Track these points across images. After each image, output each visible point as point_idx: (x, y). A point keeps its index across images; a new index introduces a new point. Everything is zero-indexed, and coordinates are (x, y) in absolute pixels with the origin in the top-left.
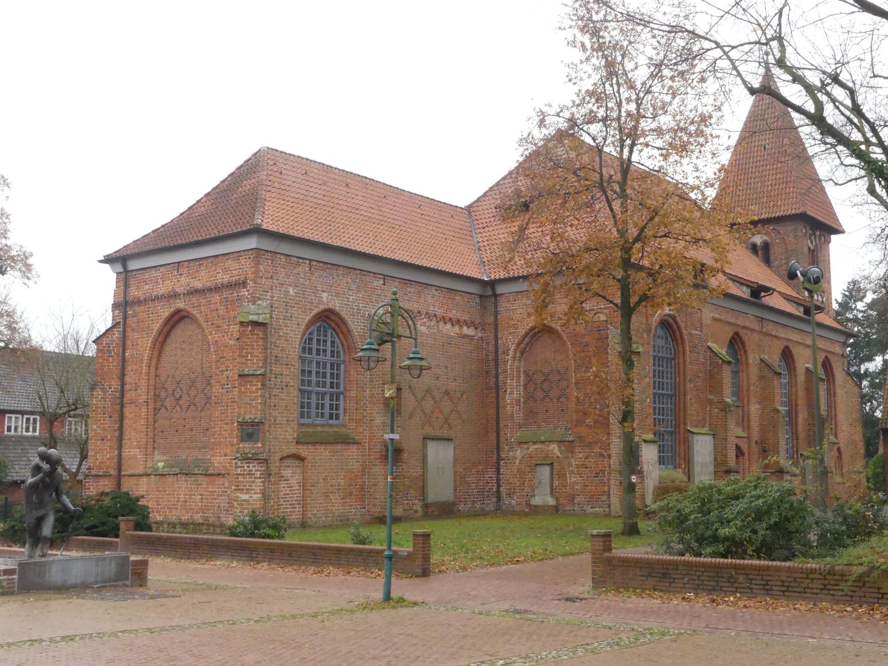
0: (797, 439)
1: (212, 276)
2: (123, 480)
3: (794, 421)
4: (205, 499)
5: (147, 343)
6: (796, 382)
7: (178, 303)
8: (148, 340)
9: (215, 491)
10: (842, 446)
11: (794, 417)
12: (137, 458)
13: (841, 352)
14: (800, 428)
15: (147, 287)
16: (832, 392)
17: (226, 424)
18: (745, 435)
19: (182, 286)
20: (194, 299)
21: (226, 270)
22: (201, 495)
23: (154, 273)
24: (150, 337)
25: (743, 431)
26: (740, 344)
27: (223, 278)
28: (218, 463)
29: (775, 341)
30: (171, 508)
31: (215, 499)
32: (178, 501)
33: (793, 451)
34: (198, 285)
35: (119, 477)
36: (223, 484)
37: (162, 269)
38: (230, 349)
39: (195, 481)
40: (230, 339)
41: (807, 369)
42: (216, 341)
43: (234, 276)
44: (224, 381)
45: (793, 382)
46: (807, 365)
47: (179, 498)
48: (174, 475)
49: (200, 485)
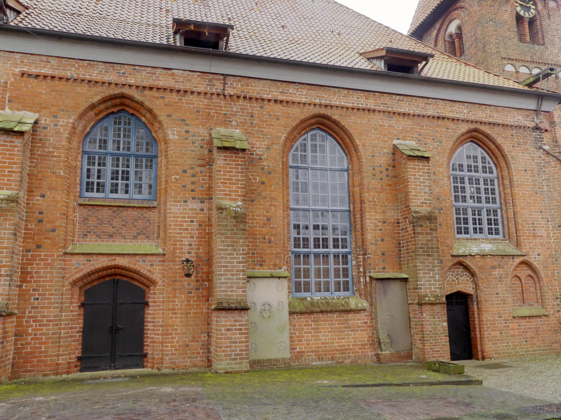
0: (365, 254)
3: (359, 227)
6: (361, 167)
10: (534, 259)
11: (358, 220)
13: (533, 125)
14: (369, 237)
16: (507, 182)
18: (160, 251)
25: (157, 246)
26: (148, 115)
29: (279, 106)
33: (359, 272)
41: (395, 147)
45: (356, 168)
46: (395, 142)
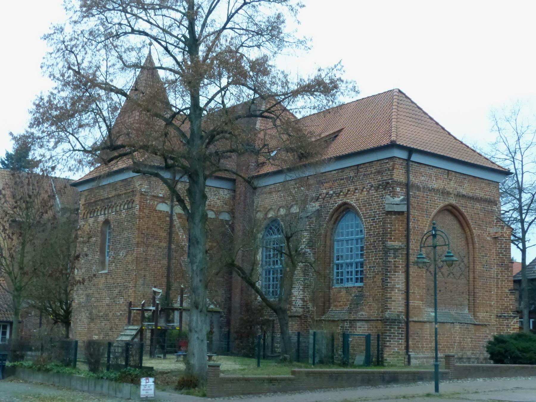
1: (472, 190)
2: (411, 325)
4: (474, 341)
5: (427, 222)
7: (451, 200)
8: (428, 220)
9: (480, 336)
12: (420, 308)
15: (423, 178)
17: (487, 291)
19: (451, 188)
20: (463, 201)
21: (482, 189)
22: (471, 338)
23: (432, 172)
24: (429, 217)
27: (479, 194)
28: (483, 317)
30: (449, 347)
31: (480, 341)
32: (455, 342)
34: (464, 193)
35: (407, 323)
36: (486, 331)
37: (435, 170)
38: (488, 243)
39: (467, 328)
40: (488, 236)
42: (479, 235)
43: (486, 195)
44: (484, 263)
47: (455, 340)
48: (451, 323)
49: (470, 331)
